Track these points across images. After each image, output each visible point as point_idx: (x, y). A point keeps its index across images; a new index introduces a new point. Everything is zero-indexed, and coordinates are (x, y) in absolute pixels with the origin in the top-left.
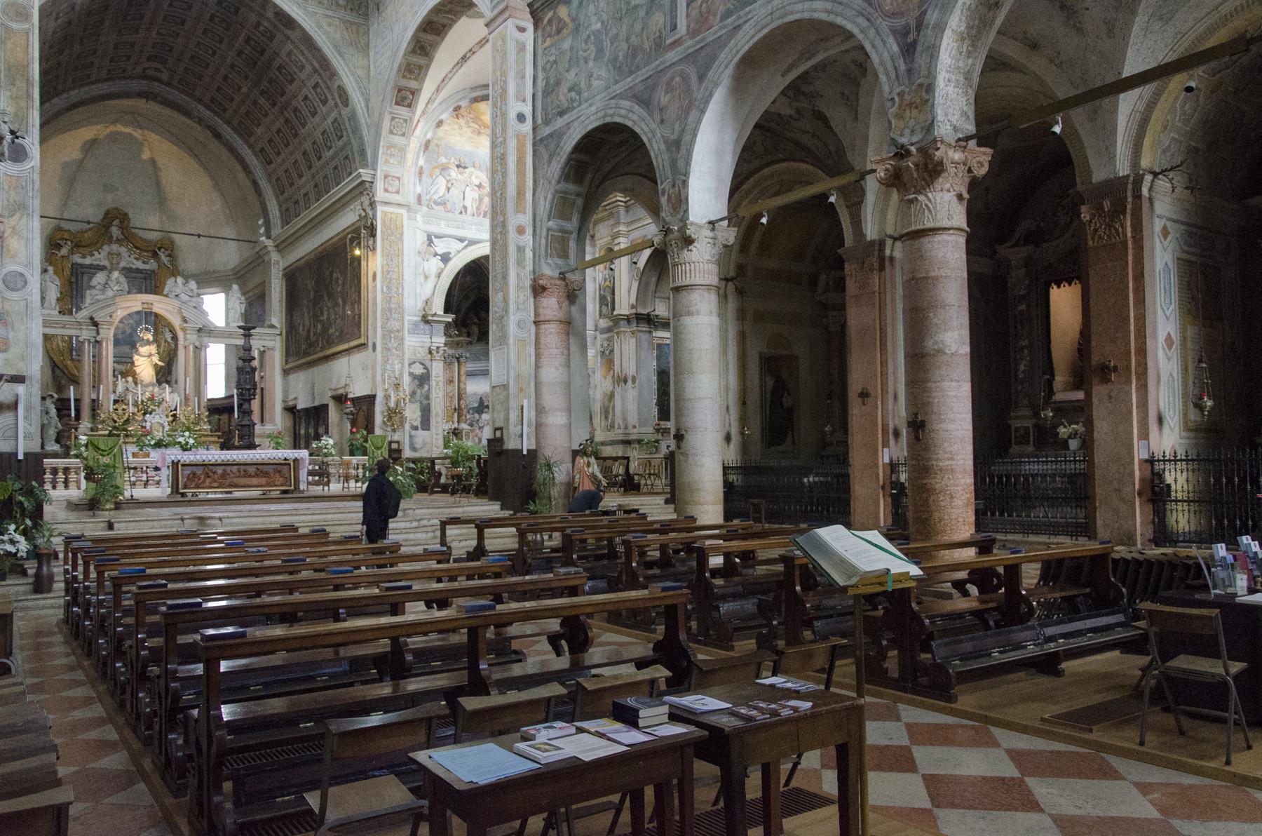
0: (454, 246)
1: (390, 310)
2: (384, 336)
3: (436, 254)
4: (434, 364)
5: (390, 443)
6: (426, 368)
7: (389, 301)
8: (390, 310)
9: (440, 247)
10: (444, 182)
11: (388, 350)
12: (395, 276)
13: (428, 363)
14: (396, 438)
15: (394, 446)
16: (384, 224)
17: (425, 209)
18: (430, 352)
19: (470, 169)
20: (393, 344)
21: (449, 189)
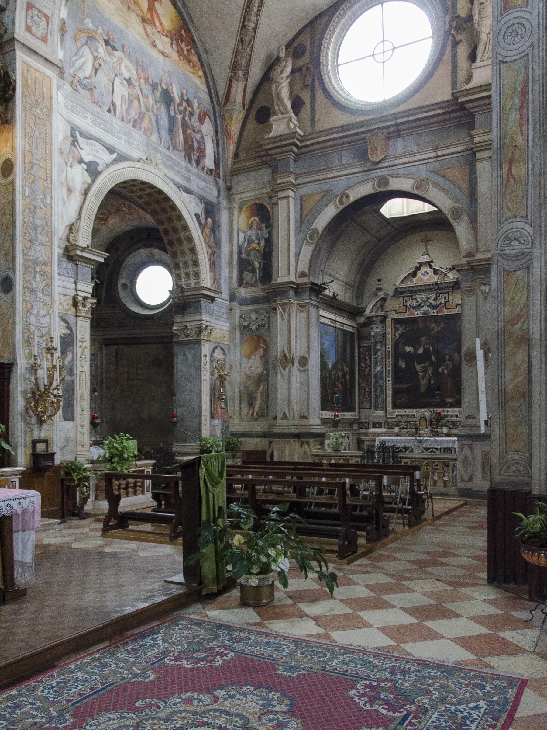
0: (105, 157)
1: (35, 228)
2: (26, 268)
3: (81, 161)
4: (80, 322)
5: (34, 443)
6: (69, 327)
7: (33, 212)
8: (35, 228)
9: (89, 151)
10: (90, 58)
11: (32, 291)
12: (41, 174)
13: (71, 320)
14: (43, 435)
15: (41, 448)
16: (25, 83)
17: (67, 87)
18: (75, 304)
19: (118, 54)
20: (38, 283)
21: (96, 71)
